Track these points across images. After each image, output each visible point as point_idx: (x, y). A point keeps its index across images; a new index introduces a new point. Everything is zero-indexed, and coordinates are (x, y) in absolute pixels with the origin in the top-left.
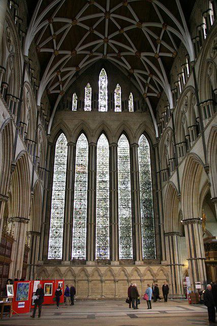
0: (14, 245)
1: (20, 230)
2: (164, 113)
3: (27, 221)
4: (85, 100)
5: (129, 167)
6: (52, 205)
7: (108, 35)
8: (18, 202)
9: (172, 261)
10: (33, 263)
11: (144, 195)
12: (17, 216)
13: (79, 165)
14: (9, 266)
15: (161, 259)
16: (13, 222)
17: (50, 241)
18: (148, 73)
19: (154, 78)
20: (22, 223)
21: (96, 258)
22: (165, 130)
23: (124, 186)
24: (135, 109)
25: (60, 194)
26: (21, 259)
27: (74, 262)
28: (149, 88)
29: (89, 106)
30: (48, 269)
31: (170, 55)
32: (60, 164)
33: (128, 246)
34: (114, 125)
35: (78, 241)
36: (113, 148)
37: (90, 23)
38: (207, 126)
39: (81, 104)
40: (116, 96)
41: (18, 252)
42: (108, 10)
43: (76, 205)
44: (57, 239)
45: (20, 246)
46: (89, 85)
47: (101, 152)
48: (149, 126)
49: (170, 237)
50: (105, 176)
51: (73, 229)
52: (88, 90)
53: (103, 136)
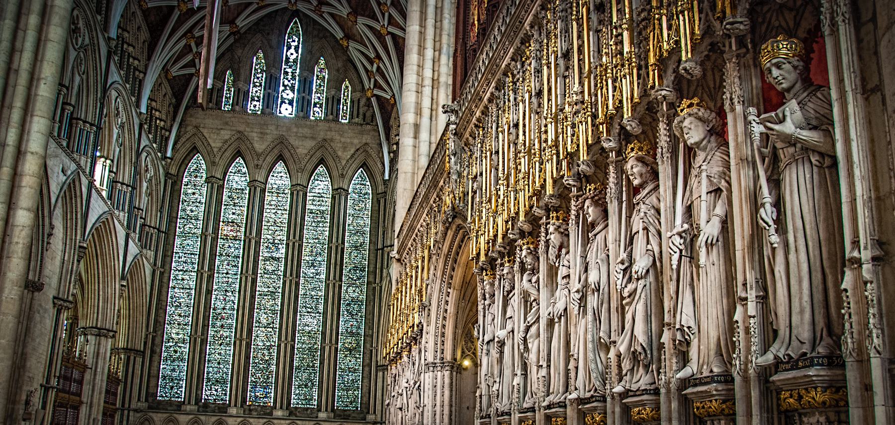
0: (88, 376)
1: (98, 350)
3: (111, 334)
4: (251, 85)
6: (169, 299)
8: (97, 301)
10: (127, 406)
11: (350, 290)
12: (94, 325)
14: (78, 410)
16: (85, 335)
18: (372, 56)
20: (102, 338)
23: (314, 271)
25: (187, 277)
26: (99, 399)
27: (205, 407)
29: (259, 101)
30: (155, 419)
33: (309, 384)
34: (303, 147)
35: (216, 370)
36: (299, 192)
39: (242, 96)
41: (93, 387)
43: (217, 301)
44: (176, 363)
45: (98, 377)
47: (274, 198)
50: (278, 249)
51: (208, 347)
53: (280, 167)
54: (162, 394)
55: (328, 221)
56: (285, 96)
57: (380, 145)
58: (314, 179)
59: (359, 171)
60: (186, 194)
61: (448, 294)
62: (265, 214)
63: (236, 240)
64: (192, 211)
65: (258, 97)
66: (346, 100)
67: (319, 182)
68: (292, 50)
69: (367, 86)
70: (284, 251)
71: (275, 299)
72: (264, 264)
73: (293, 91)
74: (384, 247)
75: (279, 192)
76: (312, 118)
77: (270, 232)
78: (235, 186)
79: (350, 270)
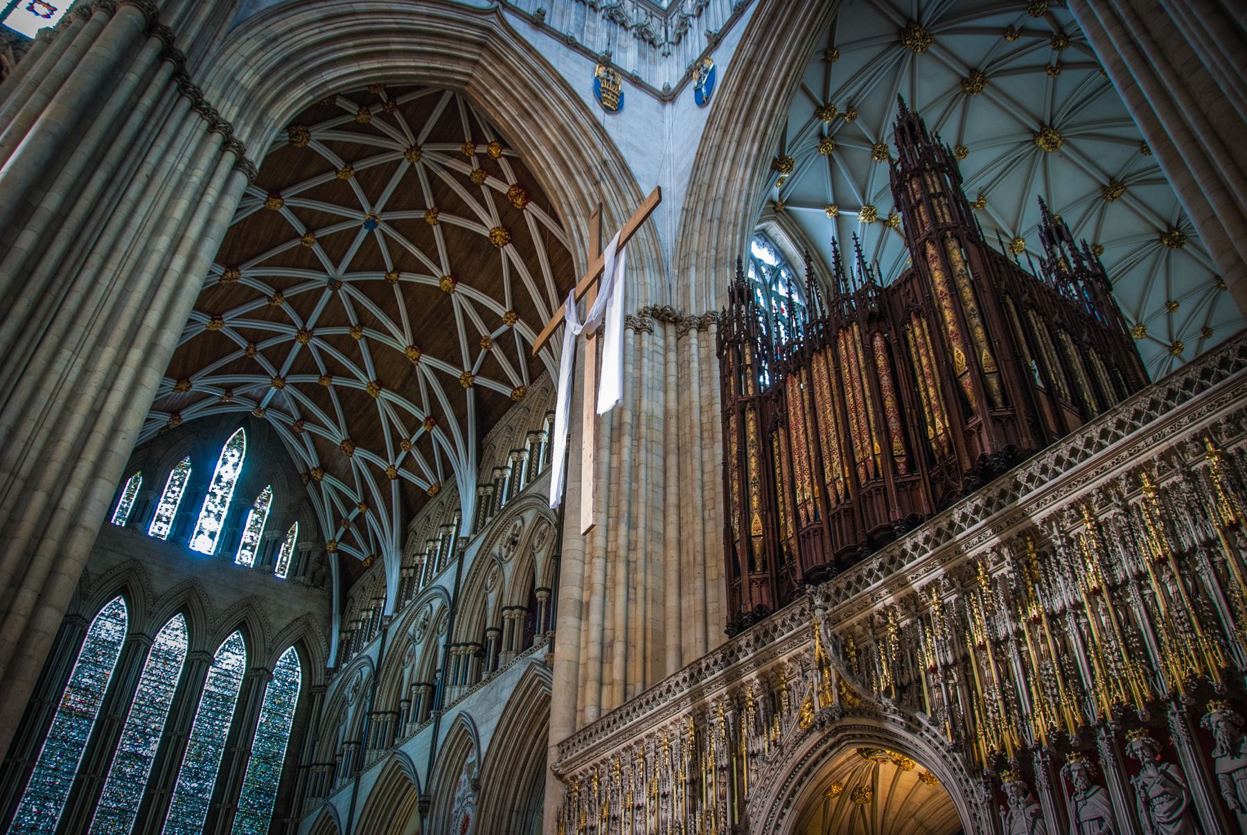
2: (368, 610)
4: (162, 499)
5: (227, 731)
7: (289, 373)
13: (77, 688)
18: (357, 499)
19: (369, 516)
22: (357, 659)
23: (195, 785)
24: (294, 571)
28: (347, 531)
29: (167, 523)
31: (425, 487)
34: (222, 601)
37: (255, 337)
38: (450, 707)
40: (252, 516)
42: (310, 326)
46: (187, 462)
47: (159, 665)
48: (318, 628)
50: (147, 743)
53: (177, 622)
55: (232, 712)
57: (329, 619)
58: (224, 649)
59: (289, 650)
61: (782, 815)
62: (140, 686)
63: (85, 718)
65: (168, 518)
66: (288, 549)
67: (230, 654)
70: (155, 747)
71: (124, 823)
72: (121, 763)
74: (311, 765)
75: (168, 656)
76: (236, 562)
77: (142, 715)
78: (103, 635)
79: (251, 793)
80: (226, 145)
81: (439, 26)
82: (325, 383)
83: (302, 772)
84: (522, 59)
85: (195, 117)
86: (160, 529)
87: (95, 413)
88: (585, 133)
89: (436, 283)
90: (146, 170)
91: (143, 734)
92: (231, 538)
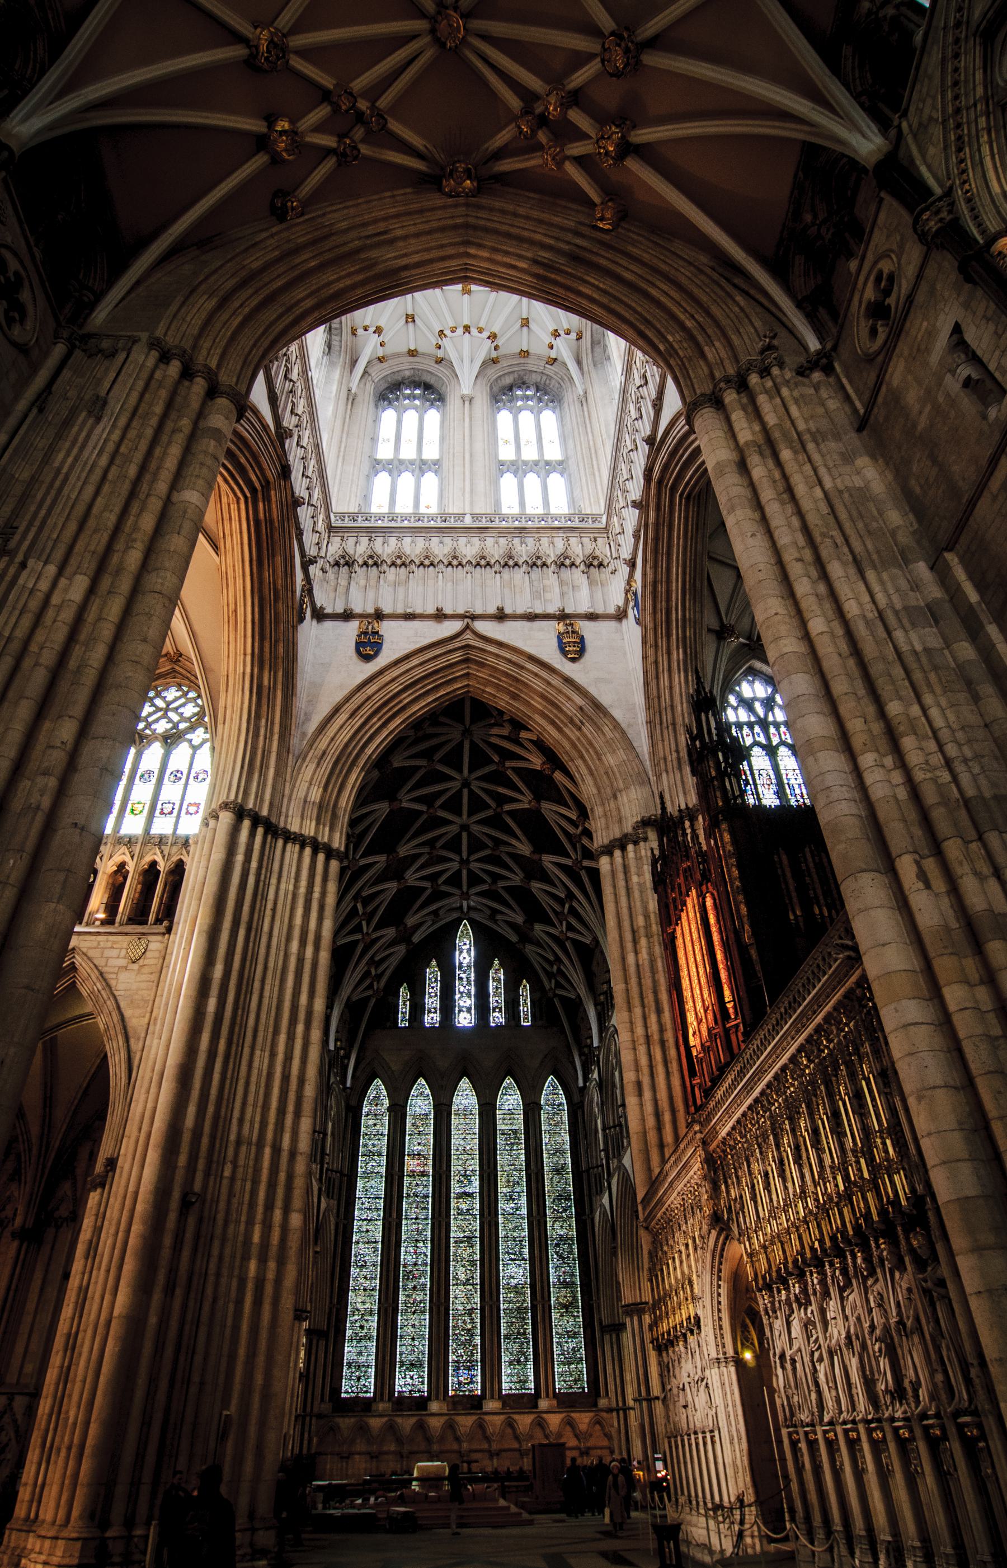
5: (523, 1157)
9: (620, 1399)
10: (308, 1410)
11: (557, 1225)
15: (598, 1395)
17: (346, 1349)
18: (552, 958)
21: (451, 1393)
25: (371, 1228)
30: (342, 1426)
32: (370, 1154)
33: (522, 1359)
37: (433, 878)
39: (418, 1009)
40: (492, 985)
43: (406, 1255)
46: (434, 963)
49: (614, 1336)
50: (470, 1182)
52: (432, 973)
53: (465, 1084)
54: (348, 1388)
56: (462, 1004)
60: (367, 1127)
64: (374, 1146)
68: (465, 954)
69: (547, 987)
70: (477, 1184)
73: (469, 997)
75: (466, 1113)
80: (316, 849)
81: (431, 667)
82: (494, 888)
83: (585, 1176)
84: (497, 656)
85: (289, 846)
86: (432, 1019)
87: (286, 1078)
88: (560, 692)
89: (527, 806)
90: (270, 905)
91: (465, 1176)
92: (482, 1008)
